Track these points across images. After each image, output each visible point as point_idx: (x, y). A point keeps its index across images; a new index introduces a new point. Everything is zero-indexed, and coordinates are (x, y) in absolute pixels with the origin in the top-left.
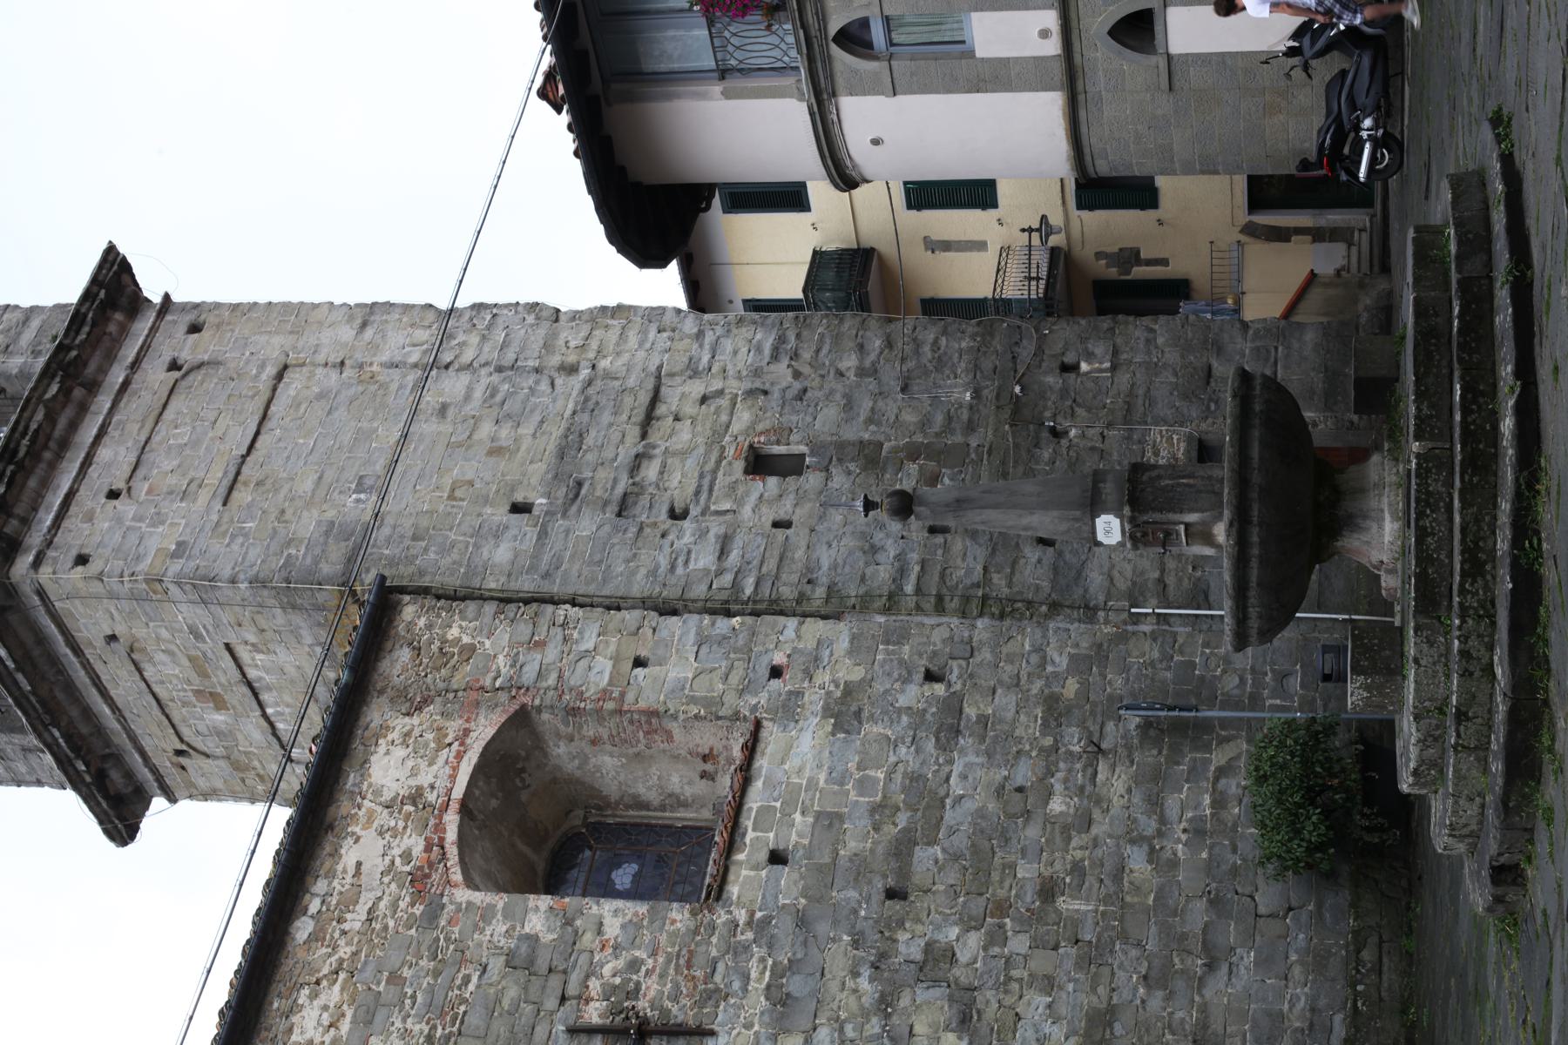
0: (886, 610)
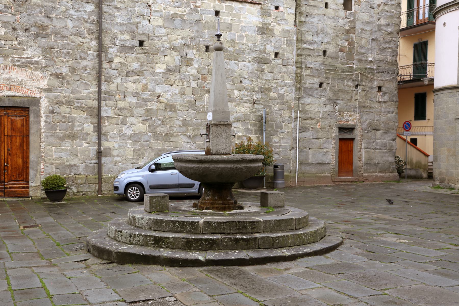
0: (298, 40)
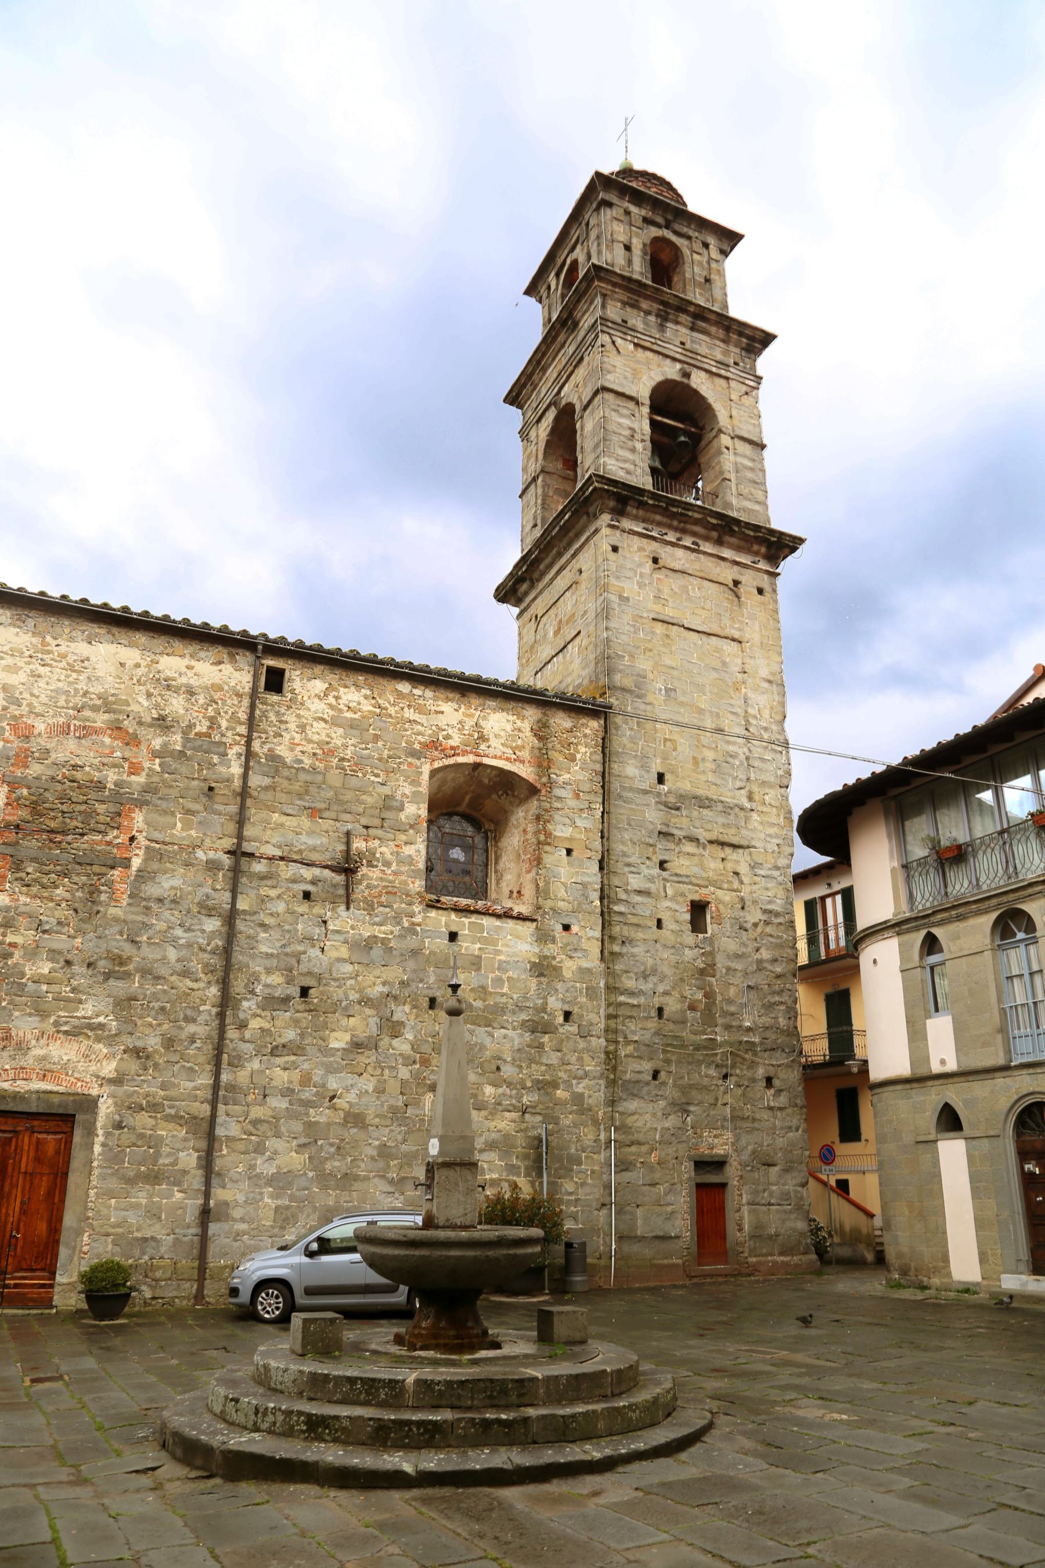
0: (608, 987)
